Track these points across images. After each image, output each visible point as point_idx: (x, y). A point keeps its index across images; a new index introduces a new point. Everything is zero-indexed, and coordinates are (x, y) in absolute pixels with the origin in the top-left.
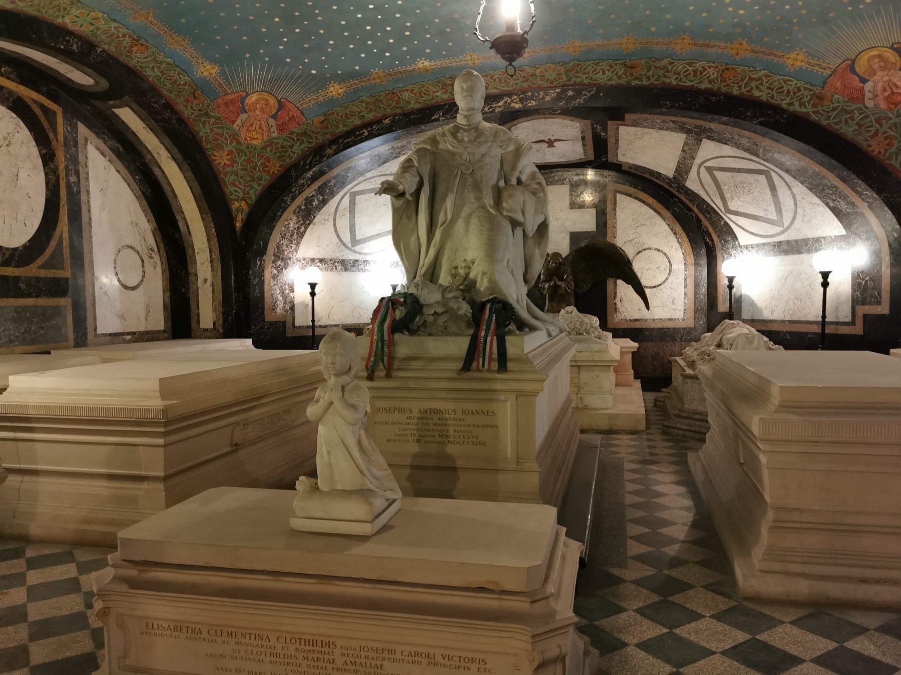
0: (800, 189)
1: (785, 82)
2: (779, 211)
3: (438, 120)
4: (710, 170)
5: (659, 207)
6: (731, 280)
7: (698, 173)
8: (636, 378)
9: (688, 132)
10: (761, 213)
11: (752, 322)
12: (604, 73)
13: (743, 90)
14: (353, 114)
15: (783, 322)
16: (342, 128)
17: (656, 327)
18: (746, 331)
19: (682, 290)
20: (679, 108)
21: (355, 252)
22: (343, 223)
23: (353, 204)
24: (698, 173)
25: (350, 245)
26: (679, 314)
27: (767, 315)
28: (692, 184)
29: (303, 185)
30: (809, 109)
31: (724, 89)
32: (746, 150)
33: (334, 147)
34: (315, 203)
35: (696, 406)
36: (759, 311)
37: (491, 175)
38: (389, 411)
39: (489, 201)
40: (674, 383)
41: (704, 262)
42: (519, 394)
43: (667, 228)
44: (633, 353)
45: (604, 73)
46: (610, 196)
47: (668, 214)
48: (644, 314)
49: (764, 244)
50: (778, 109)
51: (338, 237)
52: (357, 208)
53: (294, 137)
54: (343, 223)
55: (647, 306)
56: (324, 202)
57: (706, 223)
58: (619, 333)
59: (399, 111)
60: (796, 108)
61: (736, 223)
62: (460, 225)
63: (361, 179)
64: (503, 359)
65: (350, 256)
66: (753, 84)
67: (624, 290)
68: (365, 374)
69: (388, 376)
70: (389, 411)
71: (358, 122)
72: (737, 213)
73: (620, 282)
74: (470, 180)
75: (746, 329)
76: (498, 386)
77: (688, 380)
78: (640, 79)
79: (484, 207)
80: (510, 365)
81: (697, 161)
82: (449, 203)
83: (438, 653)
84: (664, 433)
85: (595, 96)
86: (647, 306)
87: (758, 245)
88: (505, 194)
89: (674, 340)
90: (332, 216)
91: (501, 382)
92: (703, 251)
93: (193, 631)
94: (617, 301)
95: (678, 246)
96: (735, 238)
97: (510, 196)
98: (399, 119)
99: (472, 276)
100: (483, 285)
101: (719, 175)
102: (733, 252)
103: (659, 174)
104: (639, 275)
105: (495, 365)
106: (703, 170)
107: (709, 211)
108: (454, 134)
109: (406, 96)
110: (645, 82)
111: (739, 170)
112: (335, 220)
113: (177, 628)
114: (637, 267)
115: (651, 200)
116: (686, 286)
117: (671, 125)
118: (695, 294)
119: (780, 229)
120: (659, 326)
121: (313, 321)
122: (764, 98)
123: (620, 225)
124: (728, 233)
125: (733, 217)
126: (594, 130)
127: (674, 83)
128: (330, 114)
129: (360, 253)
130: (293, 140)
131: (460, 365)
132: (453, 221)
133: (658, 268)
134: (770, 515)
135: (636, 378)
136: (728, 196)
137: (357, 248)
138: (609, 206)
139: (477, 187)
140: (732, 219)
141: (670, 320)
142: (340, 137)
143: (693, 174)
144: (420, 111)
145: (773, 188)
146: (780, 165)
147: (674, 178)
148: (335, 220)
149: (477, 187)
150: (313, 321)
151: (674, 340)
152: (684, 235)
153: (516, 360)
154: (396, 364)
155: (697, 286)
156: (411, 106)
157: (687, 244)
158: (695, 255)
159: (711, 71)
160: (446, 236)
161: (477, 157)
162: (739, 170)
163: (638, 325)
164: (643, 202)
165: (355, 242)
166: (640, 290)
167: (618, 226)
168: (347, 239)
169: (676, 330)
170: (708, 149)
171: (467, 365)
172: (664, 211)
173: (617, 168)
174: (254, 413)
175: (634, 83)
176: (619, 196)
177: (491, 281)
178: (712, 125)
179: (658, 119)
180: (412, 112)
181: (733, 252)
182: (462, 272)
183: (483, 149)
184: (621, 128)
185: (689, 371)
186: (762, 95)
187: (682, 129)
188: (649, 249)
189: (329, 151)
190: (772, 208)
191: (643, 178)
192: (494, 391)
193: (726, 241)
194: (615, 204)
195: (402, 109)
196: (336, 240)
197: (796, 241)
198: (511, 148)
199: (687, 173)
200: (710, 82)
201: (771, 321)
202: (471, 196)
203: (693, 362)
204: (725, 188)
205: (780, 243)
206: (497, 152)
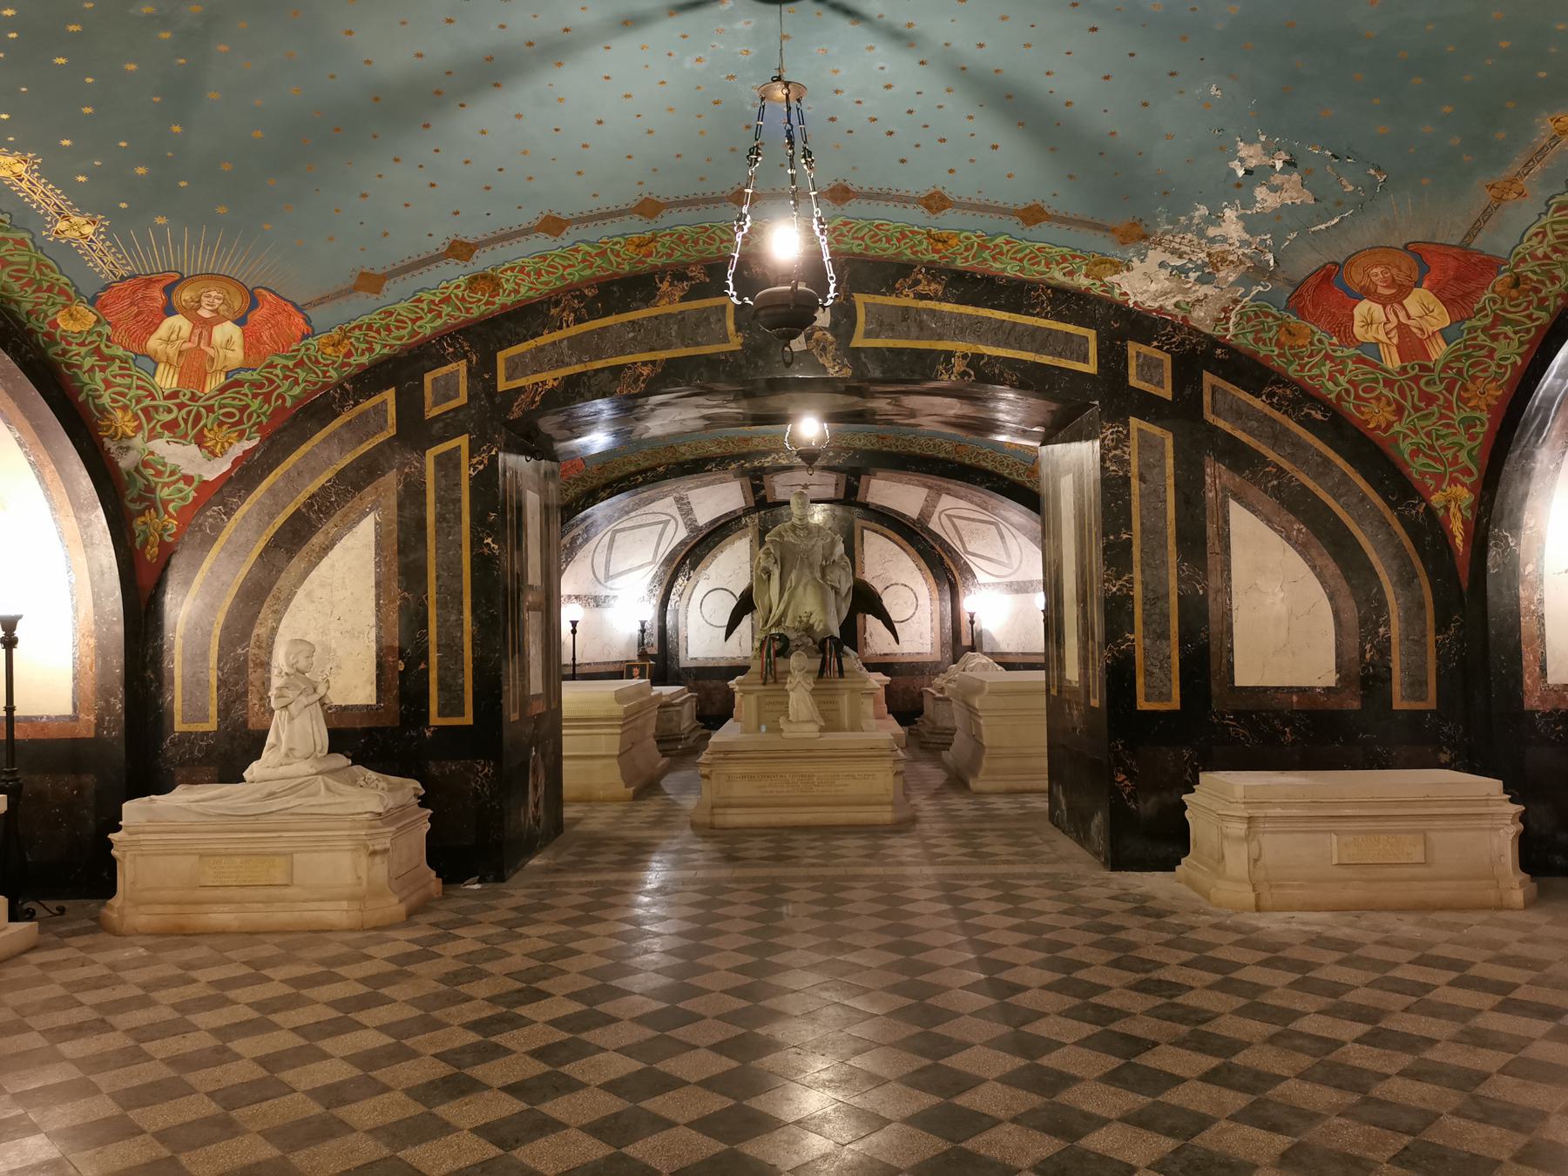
0: (1024, 540)
1: (1005, 457)
2: (1009, 556)
3: (710, 470)
4: (949, 516)
5: (904, 543)
6: (972, 616)
7: (939, 518)
8: (889, 713)
9: (930, 488)
10: (994, 557)
11: (992, 655)
12: (860, 440)
13: (973, 461)
14: (630, 462)
15: (1017, 654)
16: (617, 474)
17: (905, 661)
18: (984, 661)
19: (928, 624)
20: (922, 472)
21: (606, 587)
22: (600, 559)
23: (612, 540)
24: (939, 518)
25: (602, 581)
26: (927, 649)
27: (1004, 648)
28: (934, 525)
29: (573, 525)
30: (1024, 479)
31: (958, 459)
32: (978, 506)
33: (608, 491)
34: (580, 540)
35: (947, 724)
36: (997, 644)
37: (818, 558)
38: (774, 703)
39: (818, 575)
40: (925, 713)
41: (948, 597)
42: (853, 690)
43: (912, 564)
44: (886, 686)
45: (860, 440)
46: (857, 533)
47: (913, 551)
48: (892, 648)
49: (998, 583)
50: (1001, 477)
51: (594, 573)
52: (615, 544)
53: (571, 482)
54: (600, 559)
55: (897, 640)
56: (586, 541)
57: (947, 561)
58: (873, 667)
59: (674, 460)
60: (1015, 476)
61: (973, 562)
62: (801, 589)
63: (626, 517)
64: (841, 672)
65: (602, 592)
66: (981, 457)
67: (873, 624)
68: (761, 681)
69: (775, 682)
70: (774, 703)
71: (633, 469)
72: (974, 555)
73: (869, 617)
74: (806, 562)
75: (985, 660)
76: (840, 686)
77: (940, 702)
78: (890, 447)
79: (815, 579)
80: (845, 674)
81: (939, 509)
82: (793, 576)
83: (856, 774)
84: (921, 748)
85: (852, 458)
86: (897, 640)
87: (993, 584)
88: (828, 571)
89: (922, 673)
90: (591, 554)
91: (841, 684)
92: (947, 587)
93: (751, 777)
94: (867, 635)
95: (924, 582)
96: (974, 576)
97: (831, 572)
98: (673, 469)
99: (811, 622)
100: (818, 627)
101: (957, 521)
102: (973, 589)
103: (904, 516)
104: (888, 610)
105: (837, 675)
106: (943, 516)
107: (950, 550)
108: (794, 531)
109: (683, 449)
110: (894, 449)
111: (973, 520)
112: (593, 555)
113: (744, 777)
114: (888, 602)
115: (897, 537)
116: (932, 621)
117: (916, 482)
118: (941, 628)
119: (1011, 571)
120: (908, 660)
121: (574, 659)
122: (990, 468)
123: (867, 561)
124: (967, 571)
125: (969, 557)
126: (848, 480)
127: (918, 451)
128: (353, 328)
129: (611, 589)
130: (569, 484)
131: (817, 675)
132: (796, 587)
133: (906, 603)
134: (987, 751)
135: (889, 713)
136: (965, 539)
137: (609, 583)
138: (857, 545)
139: (811, 566)
140: (971, 561)
141: (918, 654)
142: (614, 481)
143: (935, 517)
144: (695, 461)
145: (1002, 537)
146: (1005, 519)
147: (918, 519)
148: (593, 555)
149: (811, 566)
150: (574, 659)
151: (922, 673)
152: (928, 571)
153: (848, 671)
154: (778, 676)
155: (942, 620)
156: (685, 457)
157: (931, 580)
158: (939, 591)
159: (947, 445)
160: (791, 596)
161: (810, 547)
162: (973, 520)
163: (888, 659)
164: (889, 539)
165: (608, 577)
166: (889, 624)
167: (865, 561)
168: (601, 575)
169: (925, 664)
170: (946, 502)
171: (821, 672)
172: (909, 548)
173: (865, 506)
174: (639, 721)
175: (885, 449)
176: (865, 532)
177: (825, 625)
178: (950, 486)
179: (905, 478)
180: (686, 462)
181: (973, 589)
182: (805, 619)
183: (813, 543)
184: (873, 481)
185: (938, 695)
186: (989, 466)
187: (925, 485)
188: (897, 584)
189: (603, 494)
190: (1002, 552)
191: (883, 514)
192: (837, 689)
193: (967, 579)
194: (862, 539)
195: (677, 458)
196: (592, 576)
197: (1024, 582)
198: (829, 540)
199: (930, 517)
200: (946, 453)
201: (1008, 654)
202: (807, 572)
203: (942, 688)
204: (963, 533)
205: (1011, 582)
206: (820, 543)
